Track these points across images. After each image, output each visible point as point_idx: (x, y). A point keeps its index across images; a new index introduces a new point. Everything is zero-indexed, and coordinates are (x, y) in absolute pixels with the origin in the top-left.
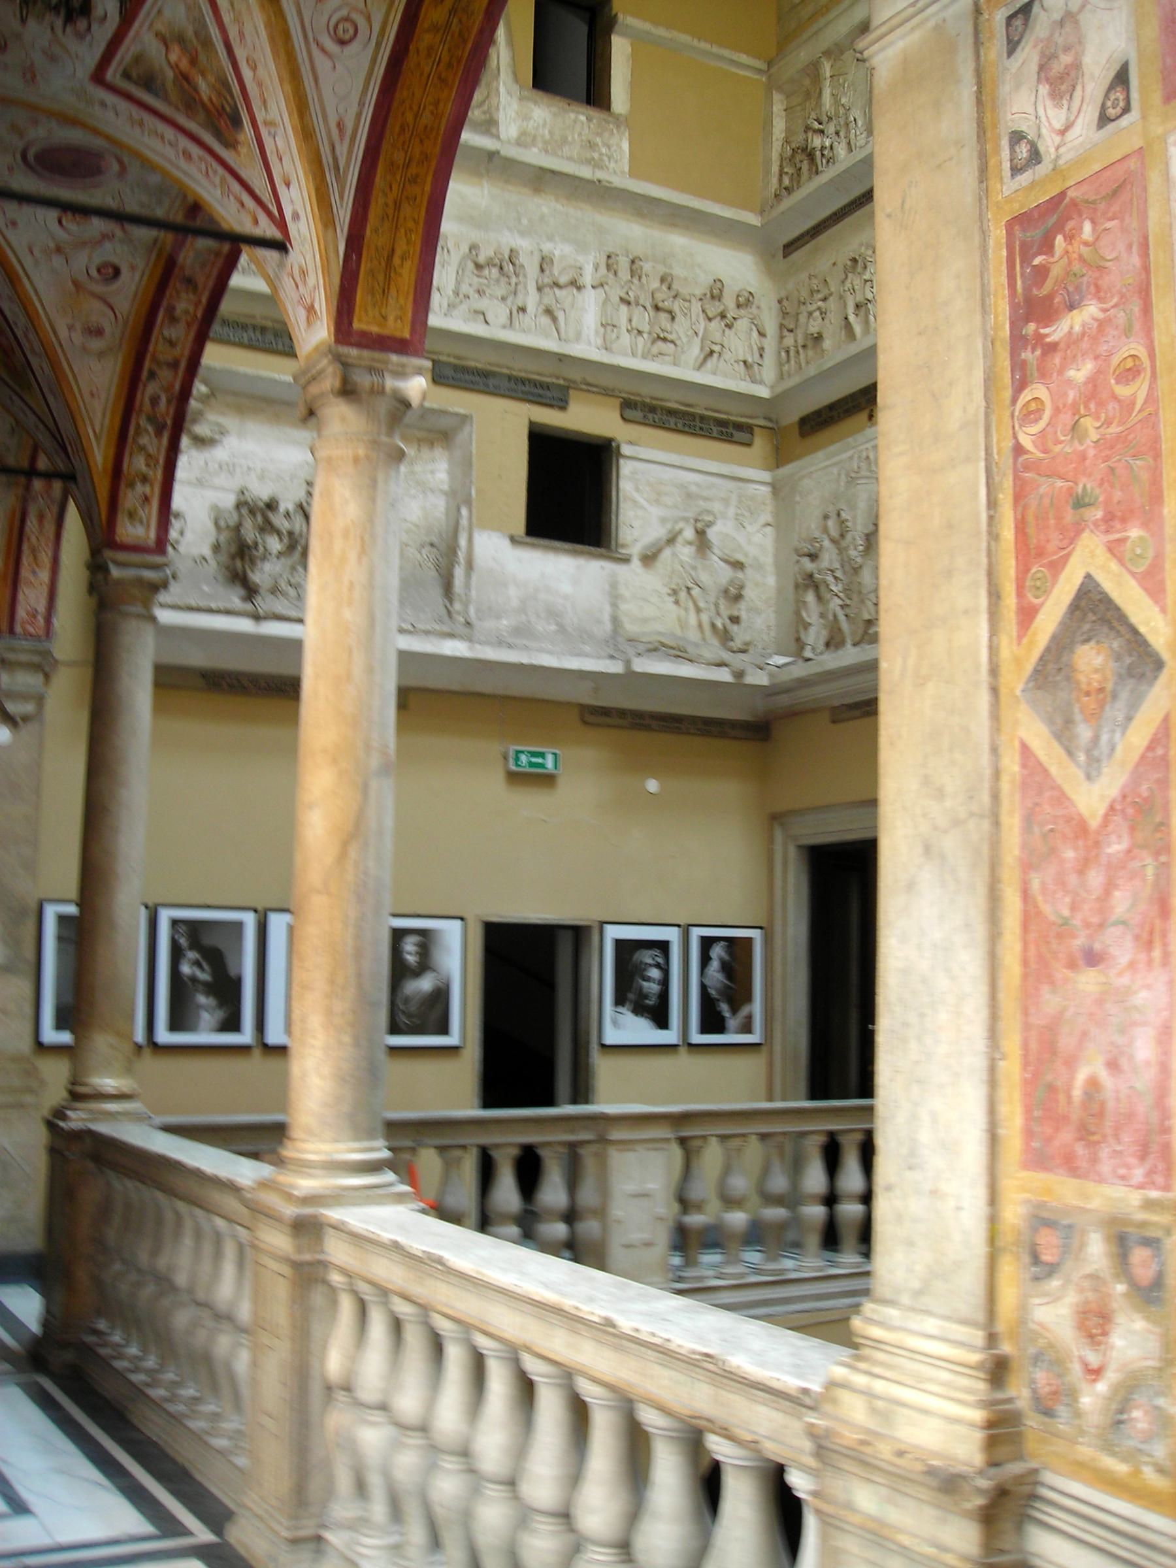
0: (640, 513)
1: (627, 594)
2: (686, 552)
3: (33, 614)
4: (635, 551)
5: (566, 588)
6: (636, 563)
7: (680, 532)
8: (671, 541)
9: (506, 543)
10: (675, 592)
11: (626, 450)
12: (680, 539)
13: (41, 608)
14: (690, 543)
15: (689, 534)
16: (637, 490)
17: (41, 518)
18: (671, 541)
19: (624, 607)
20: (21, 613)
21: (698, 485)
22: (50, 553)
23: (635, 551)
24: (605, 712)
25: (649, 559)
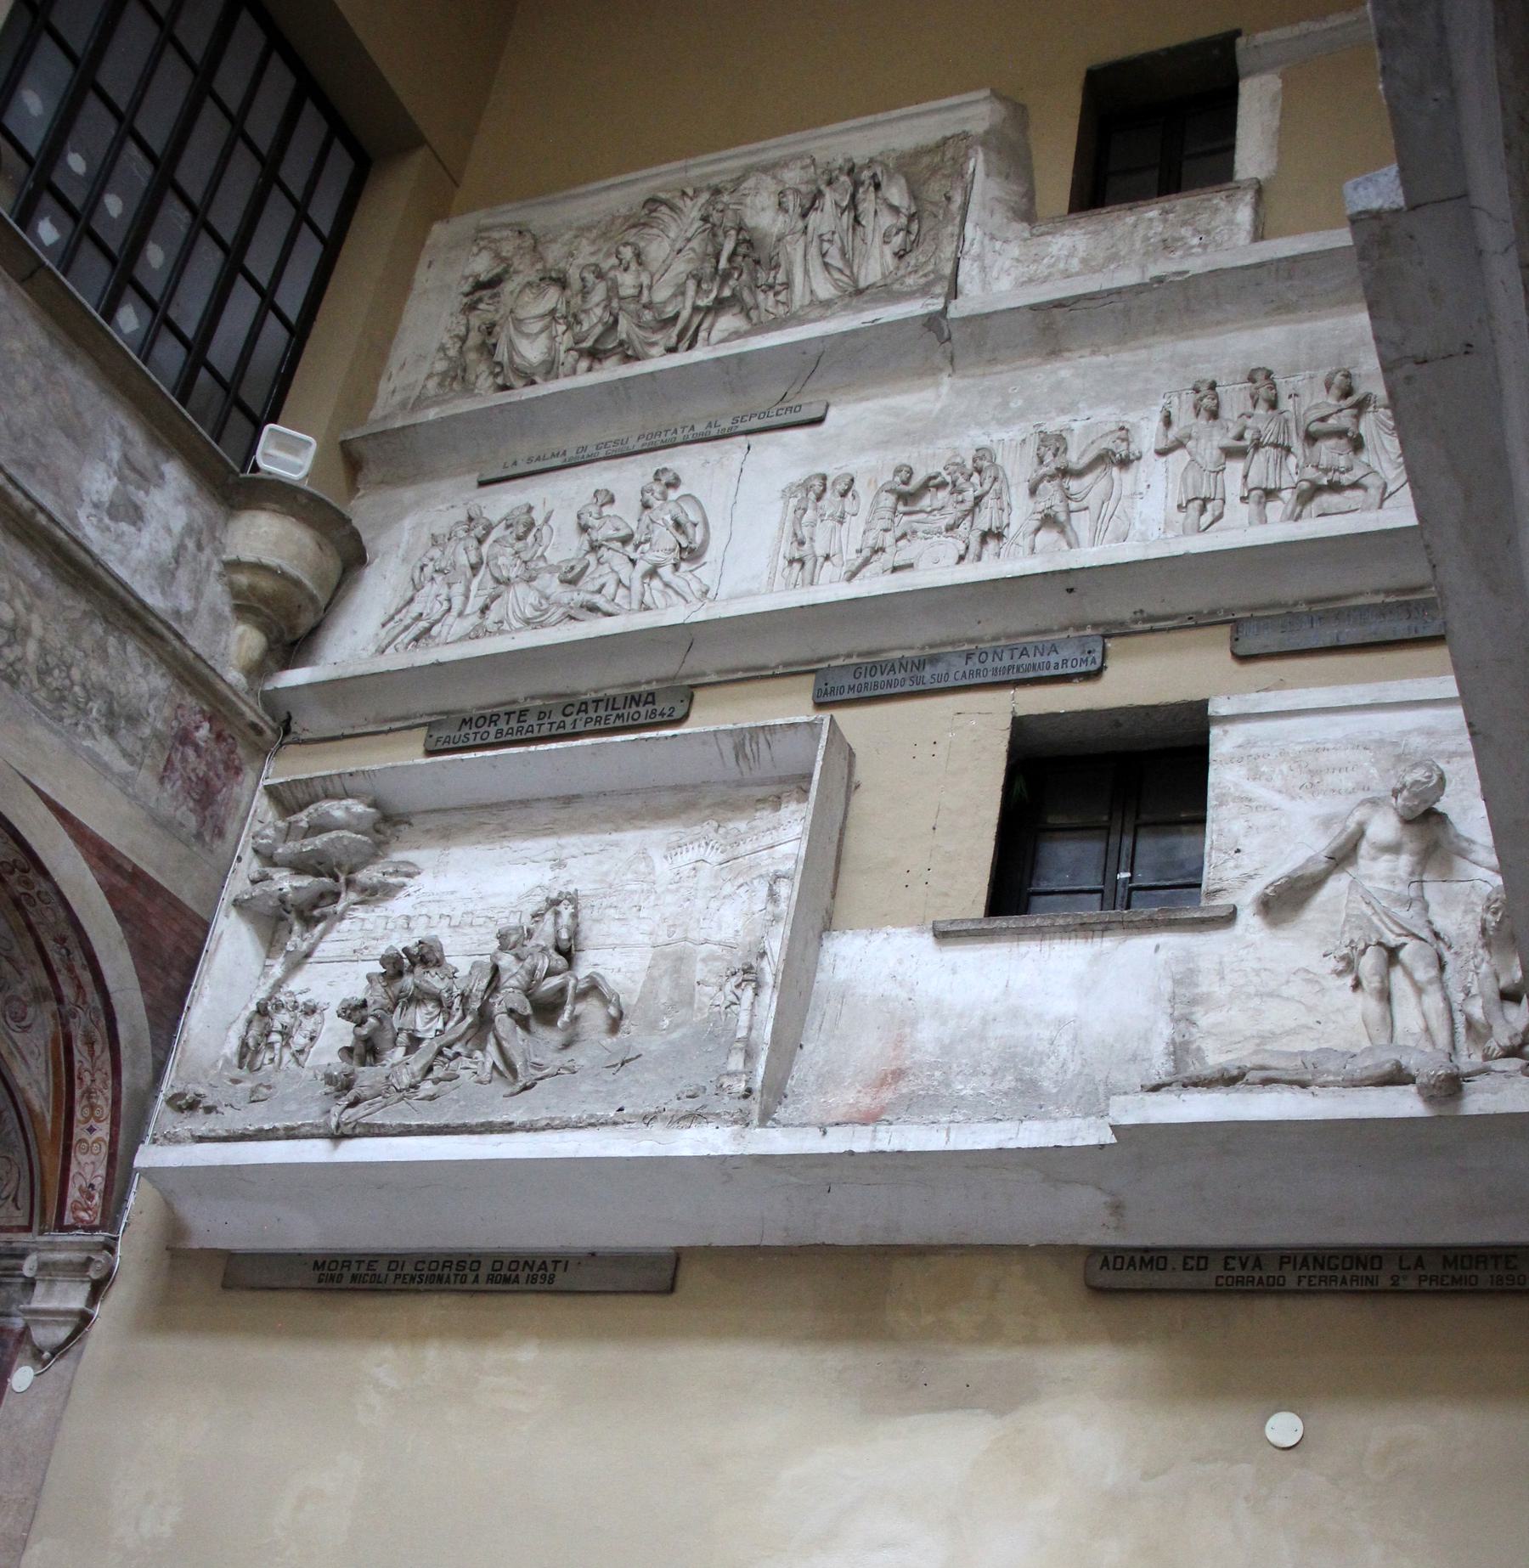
0: (1261, 819)
1: (1220, 991)
2: (1383, 872)
3: (88, 1191)
4: (1245, 900)
5: (1065, 1005)
6: (1248, 919)
7: (1360, 833)
8: (1343, 856)
9: (928, 939)
10: (1349, 964)
11: (1218, 707)
12: (1364, 848)
13: (99, 1183)
14: (1394, 849)
15: (1384, 827)
16: (1255, 775)
17: (90, 1043)
18: (1343, 856)
19: (1205, 1019)
20: (73, 1194)
21: (1429, 733)
22: (108, 1093)
23: (1245, 900)
24: (1151, 1258)
25: (1286, 900)
